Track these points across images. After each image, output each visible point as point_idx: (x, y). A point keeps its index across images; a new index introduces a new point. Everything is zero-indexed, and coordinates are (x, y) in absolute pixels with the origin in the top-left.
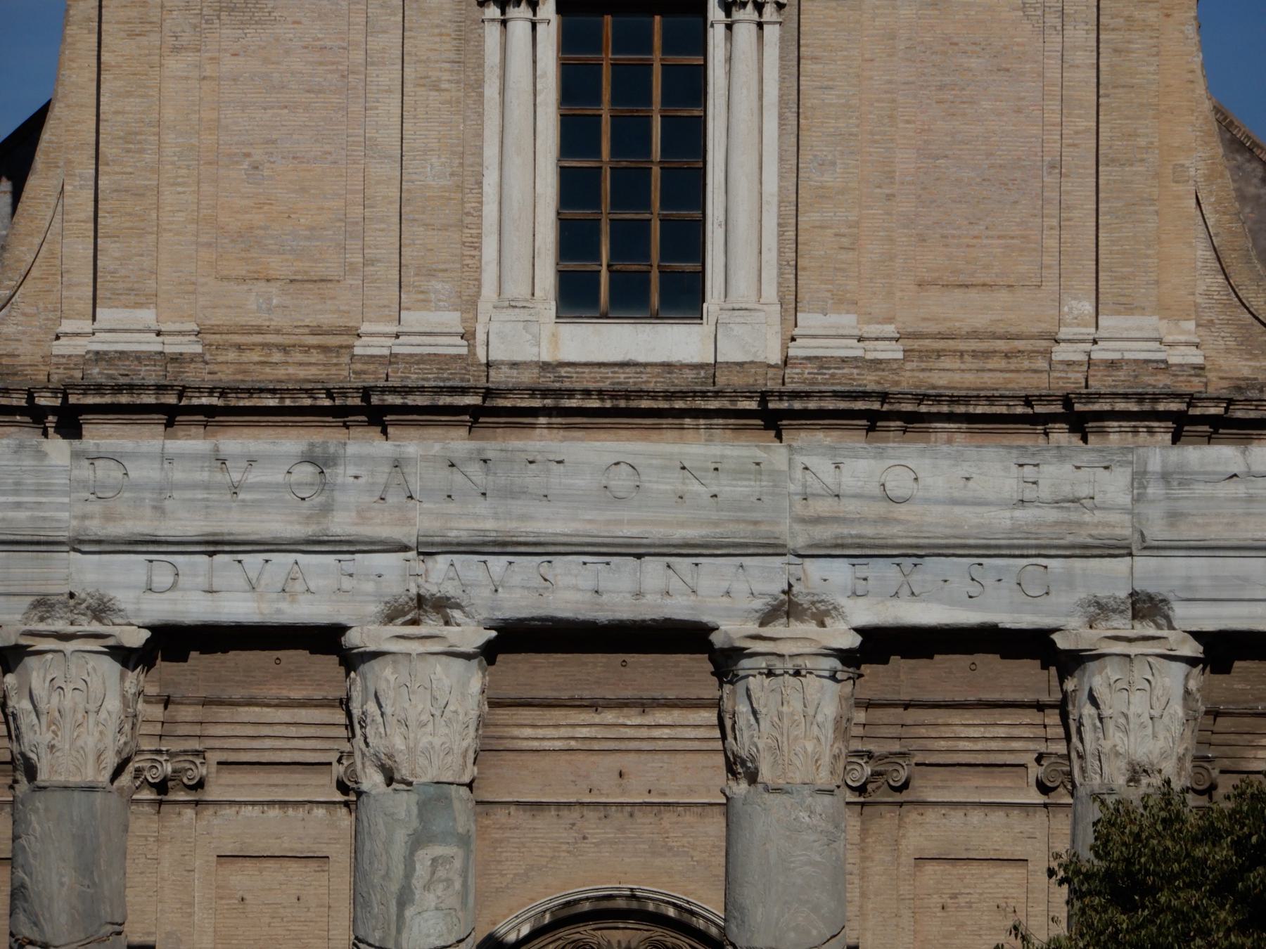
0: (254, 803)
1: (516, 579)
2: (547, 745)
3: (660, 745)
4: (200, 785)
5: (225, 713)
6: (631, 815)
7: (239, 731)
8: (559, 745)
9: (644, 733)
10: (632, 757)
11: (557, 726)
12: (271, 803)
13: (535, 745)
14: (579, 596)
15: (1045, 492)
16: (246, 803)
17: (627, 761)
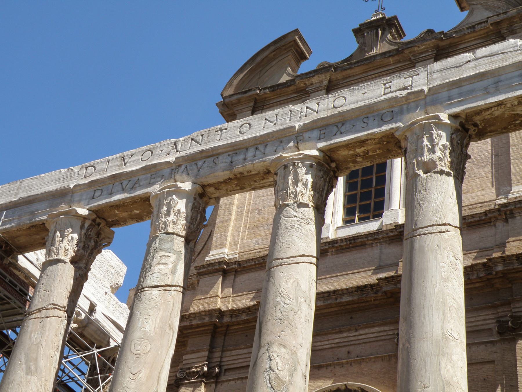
0: (233, 380)
1: (206, 165)
2: (325, 347)
3: (362, 341)
4: (218, 375)
5: (228, 354)
6: (351, 365)
7: (232, 358)
8: (329, 346)
9: (356, 338)
10: (352, 347)
11: (328, 340)
12: (238, 379)
13: (321, 347)
14: (225, 164)
15: (393, 89)
16: (230, 380)
17: (351, 348)
